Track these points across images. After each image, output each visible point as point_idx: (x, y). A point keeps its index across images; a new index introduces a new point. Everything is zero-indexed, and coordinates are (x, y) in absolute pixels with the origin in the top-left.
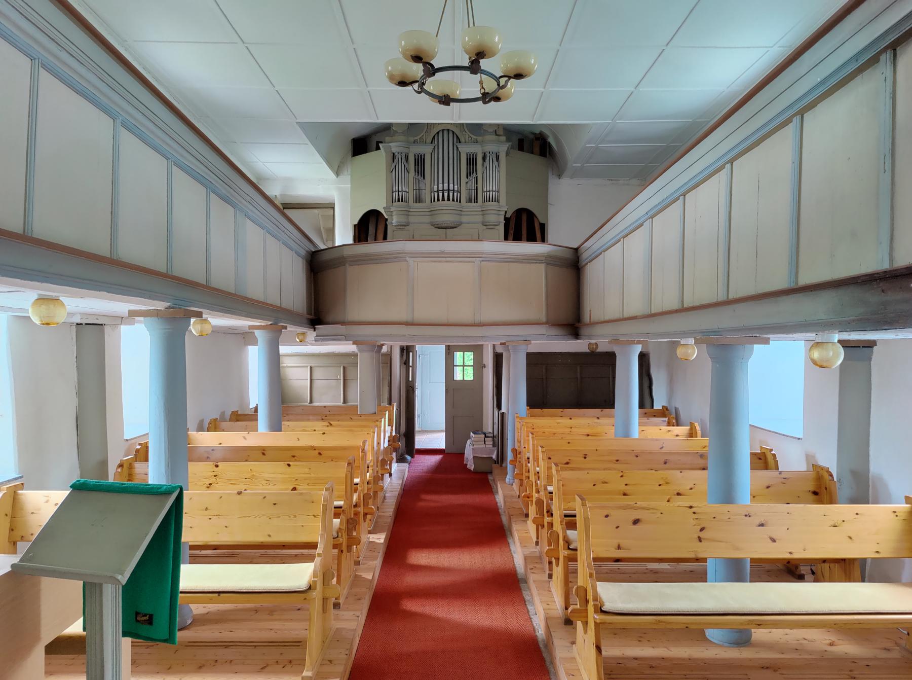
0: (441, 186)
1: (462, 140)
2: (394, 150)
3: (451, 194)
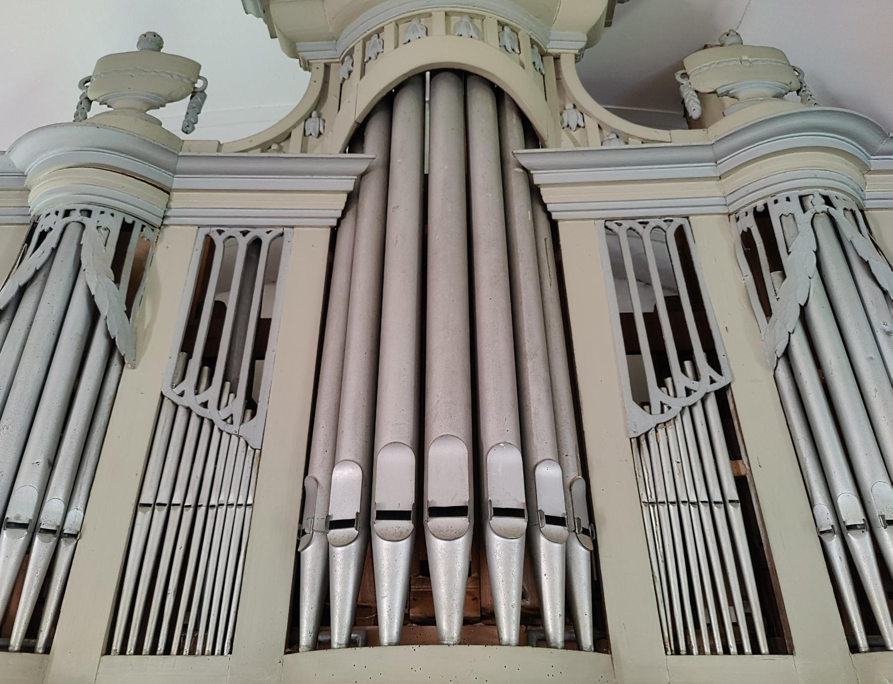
0: (394, 463)
3: (504, 554)
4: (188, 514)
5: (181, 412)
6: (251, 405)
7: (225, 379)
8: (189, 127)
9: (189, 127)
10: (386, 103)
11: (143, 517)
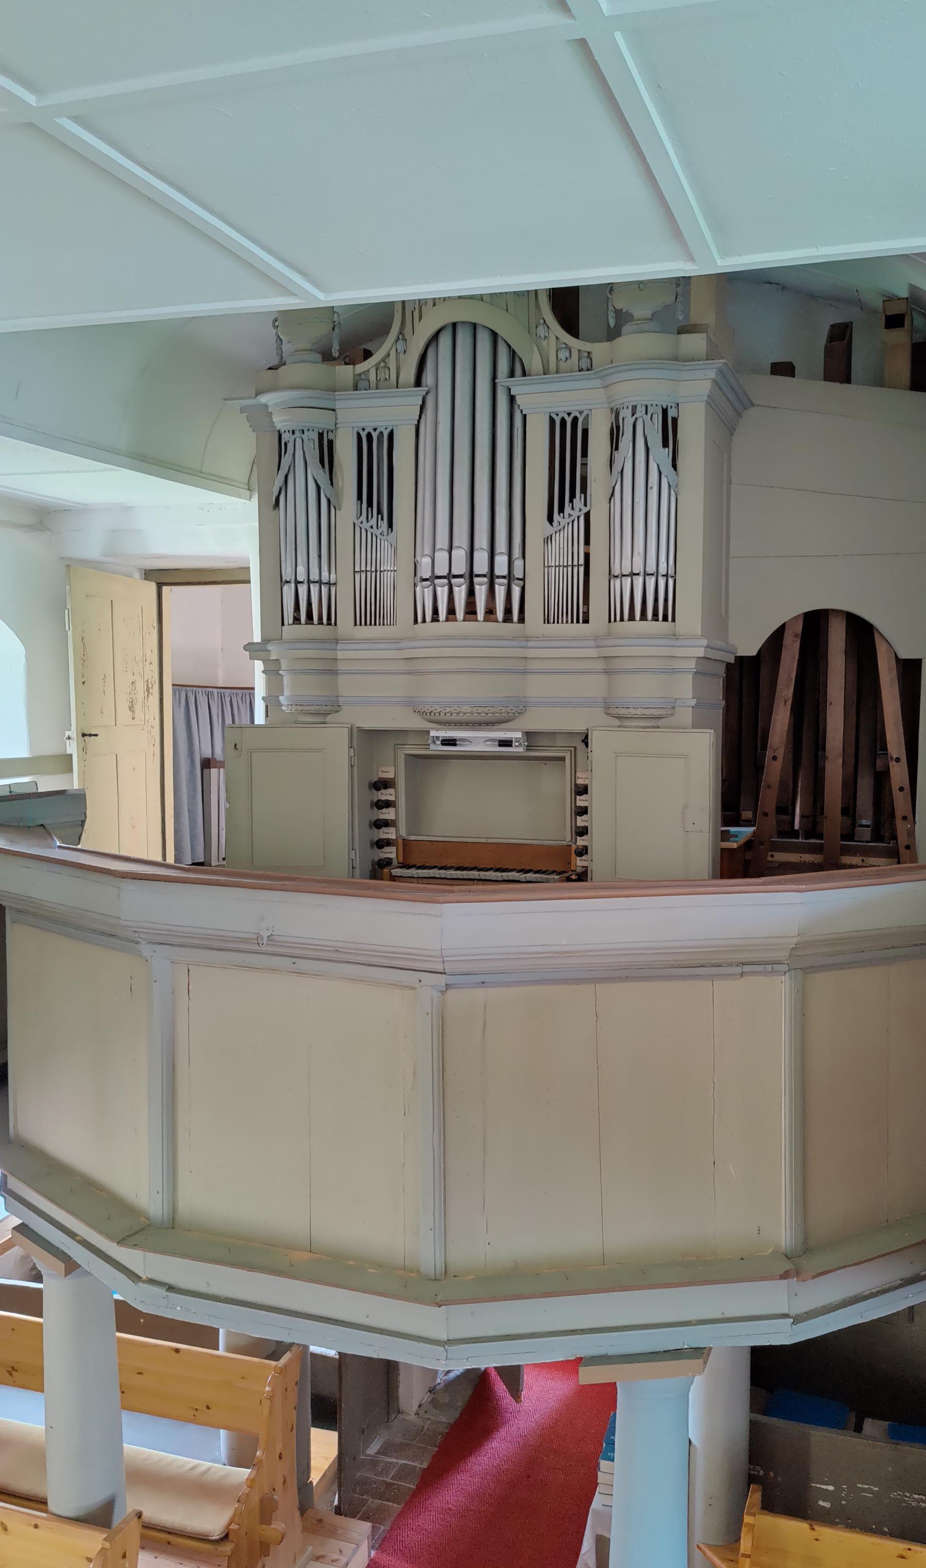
1: (534, 363)
2: (280, 421)
4: (374, 574)
5: (363, 531)
6: (390, 525)
7: (378, 514)
10: (435, 337)
11: (357, 576)
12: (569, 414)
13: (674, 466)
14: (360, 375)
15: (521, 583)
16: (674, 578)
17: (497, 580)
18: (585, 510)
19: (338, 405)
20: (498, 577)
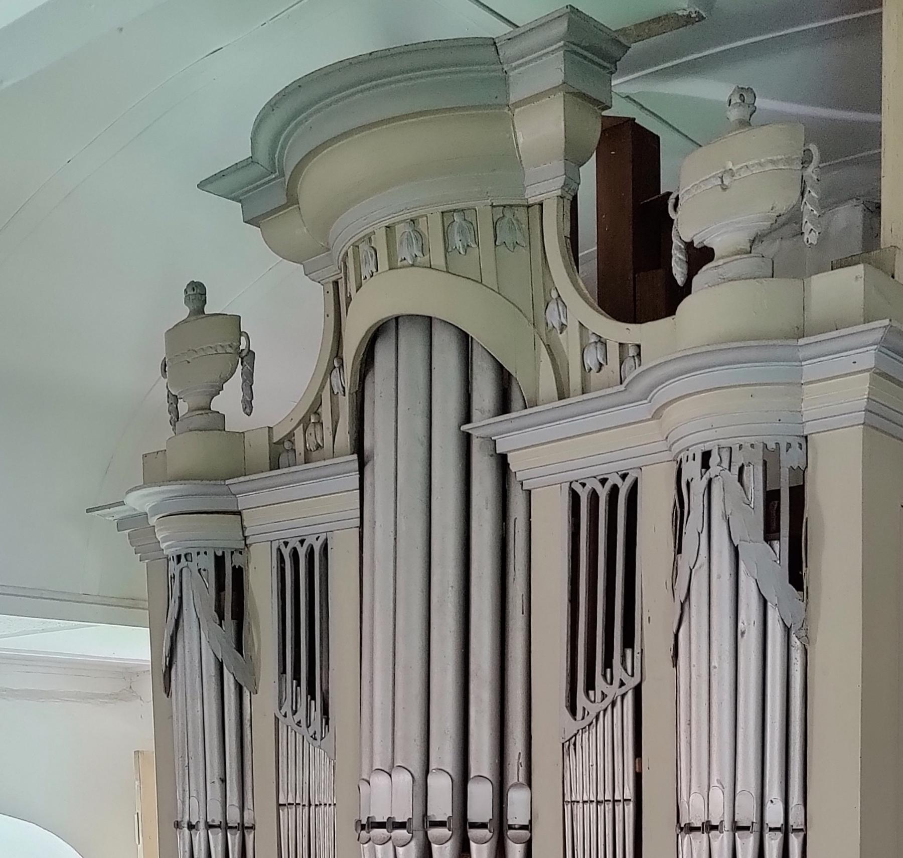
8: (248, 406)
9: (248, 406)
12: (603, 481)
13: (796, 579)
14: (281, 442)
15: (524, 833)
16: (803, 831)
17: (473, 833)
18: (632, 683)
19: (242, 503)
20: (475, 826)
